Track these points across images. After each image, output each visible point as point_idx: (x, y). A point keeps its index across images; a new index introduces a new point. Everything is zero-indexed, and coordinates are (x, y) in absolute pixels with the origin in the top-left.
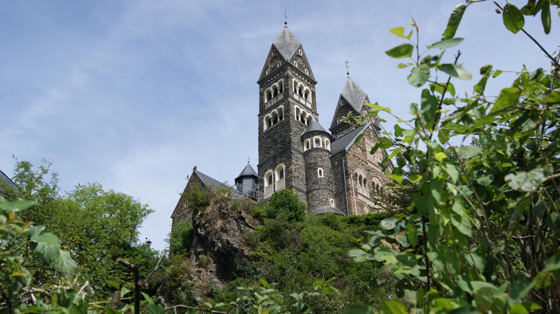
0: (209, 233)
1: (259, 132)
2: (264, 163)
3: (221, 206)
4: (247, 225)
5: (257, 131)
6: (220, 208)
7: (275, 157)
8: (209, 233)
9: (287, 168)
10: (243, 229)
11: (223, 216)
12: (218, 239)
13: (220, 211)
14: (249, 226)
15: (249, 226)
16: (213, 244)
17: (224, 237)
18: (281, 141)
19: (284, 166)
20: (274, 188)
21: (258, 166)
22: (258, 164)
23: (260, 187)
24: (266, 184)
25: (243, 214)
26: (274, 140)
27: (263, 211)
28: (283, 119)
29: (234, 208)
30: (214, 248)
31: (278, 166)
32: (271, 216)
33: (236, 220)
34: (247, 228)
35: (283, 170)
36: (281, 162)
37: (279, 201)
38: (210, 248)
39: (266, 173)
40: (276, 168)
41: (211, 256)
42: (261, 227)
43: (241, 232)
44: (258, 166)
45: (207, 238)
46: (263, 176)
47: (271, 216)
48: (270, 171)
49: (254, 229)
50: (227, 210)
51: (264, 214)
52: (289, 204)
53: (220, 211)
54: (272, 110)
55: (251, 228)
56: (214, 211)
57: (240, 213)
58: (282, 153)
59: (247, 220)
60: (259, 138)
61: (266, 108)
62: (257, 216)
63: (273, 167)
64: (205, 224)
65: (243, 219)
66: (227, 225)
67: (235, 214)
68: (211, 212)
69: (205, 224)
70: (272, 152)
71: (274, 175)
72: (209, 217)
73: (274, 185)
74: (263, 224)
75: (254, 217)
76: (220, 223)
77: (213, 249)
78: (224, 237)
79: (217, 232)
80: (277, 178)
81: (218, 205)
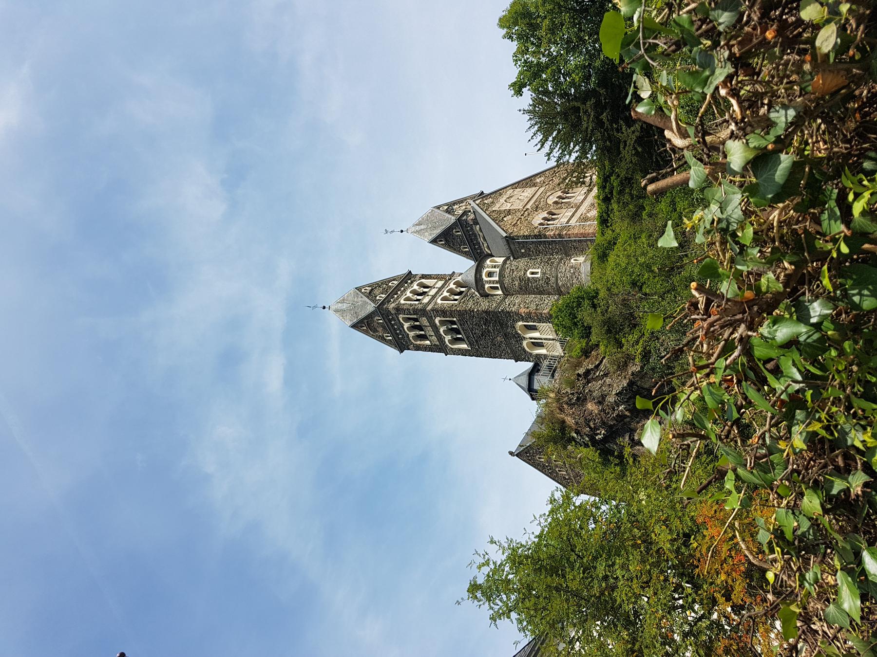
0: (603, 423)
3: (567, 403)
4: (597, 367)
6: (571, 405)
8: (603, 423)
9: (523, 320)
10: (602, 373)
11: (581, 400)
12: (614, 410)
13: (574, 404)
14: (599, 365)
15: (599, 365)
16: (621, 417)
17: (611, 399)
19: (520, 323)
25: (581, 371)
27: (578, 345)
29: (572, 385)
30: (627, 416)
32: (587, 332)
33: (588, 382)
34: (602, 367)
37: (567, 322)
38: (625, 424)
41: (638, 423)
42: (602, 348)
43: (606, 375)
45: (611, 427)
47: (587, 332)
49: (604, 357)
50: (573, 394)
51: (584, 342)
52: (573, 308)
53: (574, 404)
55: (601, 362)
56: (573, 413)
57: (579, 375)
59: (591, 367)
62: (586, 353)
64: (590, 428)
65: (588, 372)
66: (594, 394)
67: (580, 383)
68: (575, 418)
69: (590, 428)
72: (582, 420)
74: (597, 346)
75: (587, 357)
76: (591, 406)
77: (628, 419)
78: (611, 399)
79: (604, 410)
81: (565, 406)
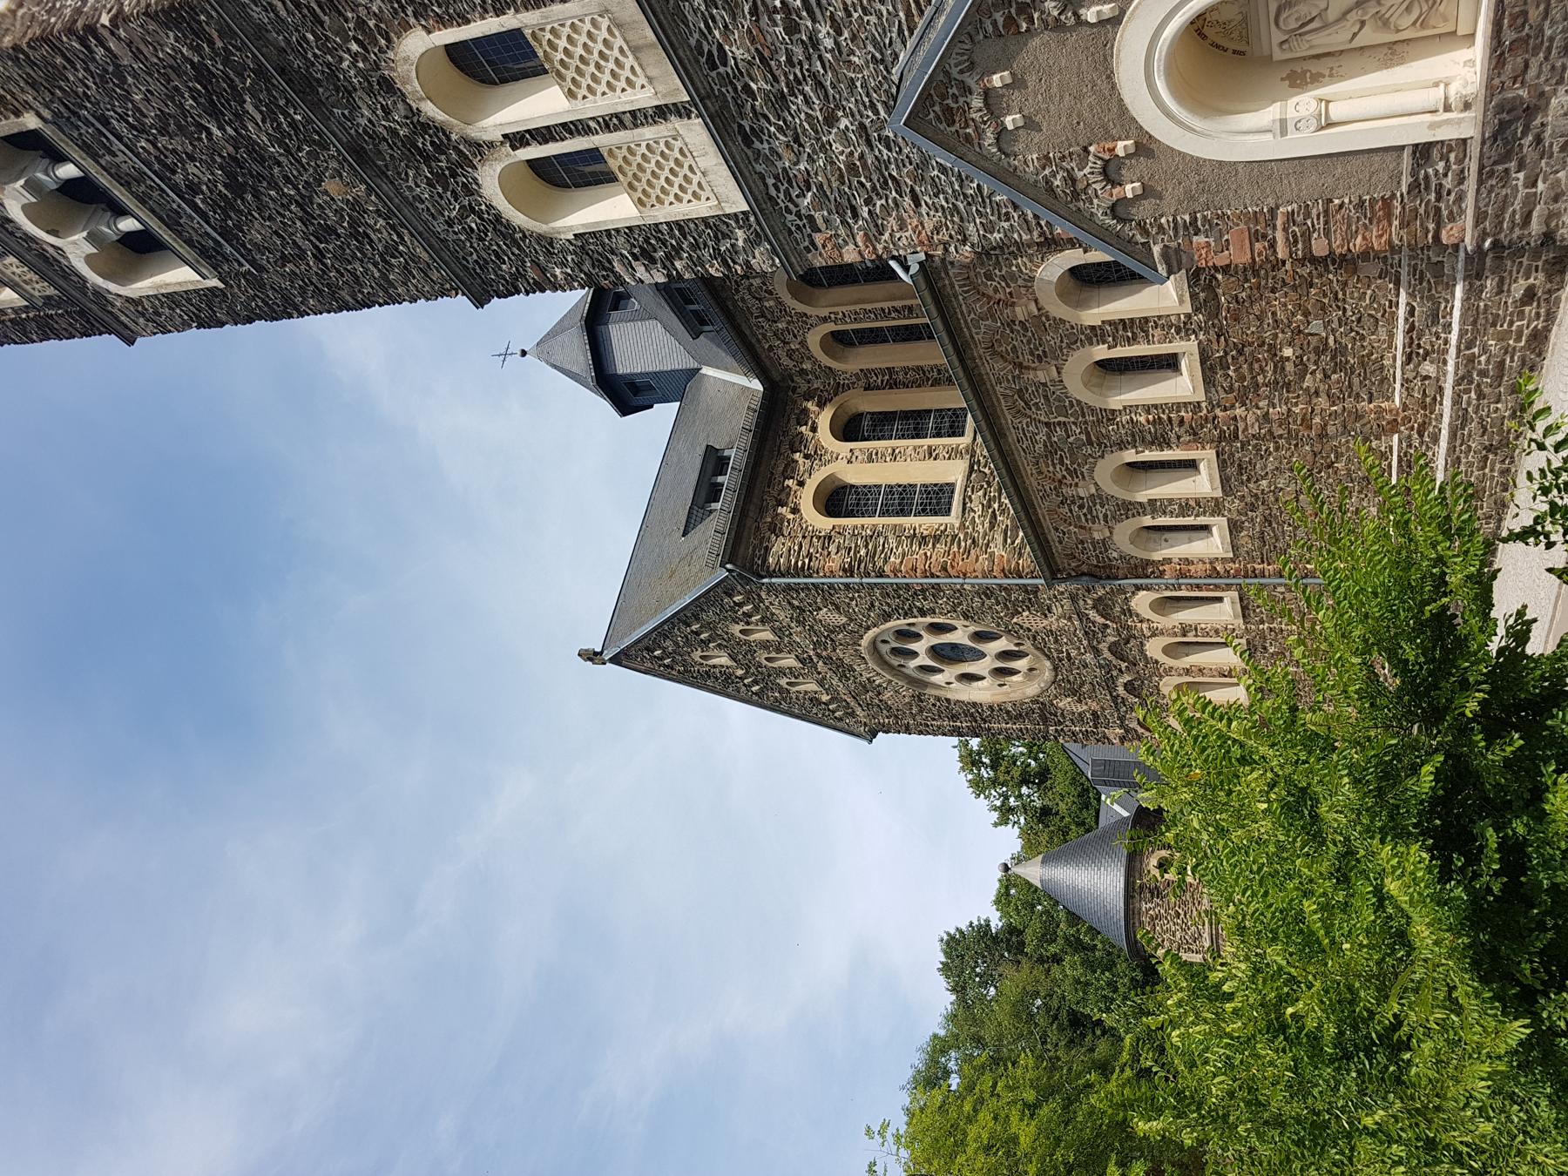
1: (209, 321)
2: (437, 245)
5: (196, 338)
7: (361, 154)
18: (215, 114)
20: (637, 118)
21: (480, 301)
22: (462, 302)
23: (647, 257)
24: (611, 210)
26: (237, 189)
28: (31, 122)
31: (430, 110)
35: (455, 52)
36: (388, 86)
39: (518, 218)
40: (457, 128)
44: (480, 301)
46: (547, 242)
48: (490, 180)
54: (29, 238)
58: (305, 87)
60: (274, 317)
61: (51, 291)
63: (452, 160)
70: (331, 186)
71: (517, 140)
73: (613, 122)
80: (541, 104)
